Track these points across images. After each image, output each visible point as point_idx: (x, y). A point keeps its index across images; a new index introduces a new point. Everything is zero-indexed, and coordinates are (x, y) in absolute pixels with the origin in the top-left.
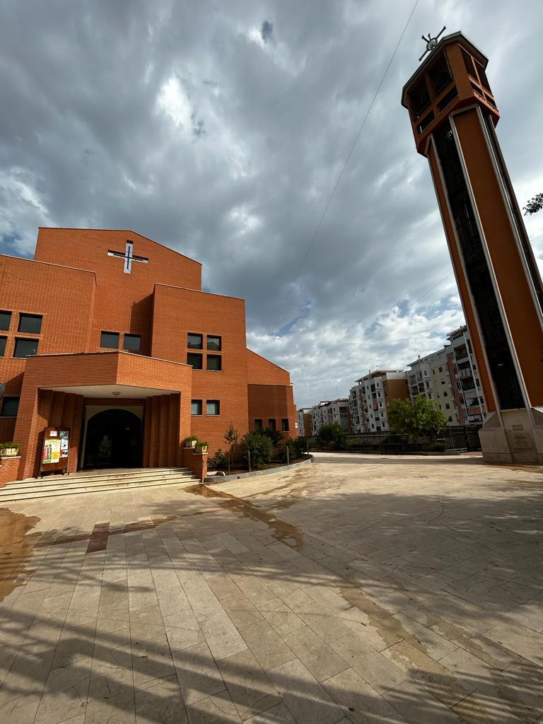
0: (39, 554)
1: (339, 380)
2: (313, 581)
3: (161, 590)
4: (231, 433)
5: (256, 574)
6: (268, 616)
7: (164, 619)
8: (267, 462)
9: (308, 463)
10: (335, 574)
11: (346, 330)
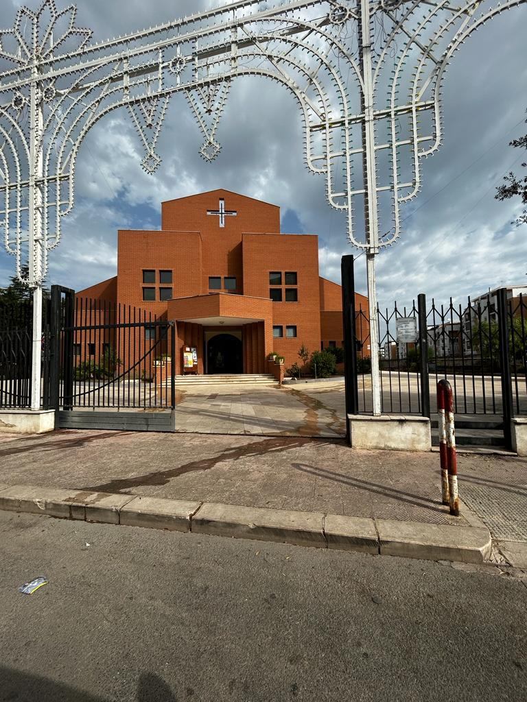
4: (303, 351)
11: (465, 237)
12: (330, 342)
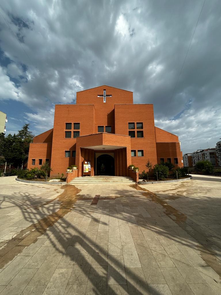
0: (78, 202)
1: (210, 139)
2: (183, 242)
3: (111, 225)
4: (148, 164)
5: (152, 229)
6: (154, 253)
7: (109, 239)
8: (166, 177)
9: (188, 179)
10: (198, 242)
11: (214, 112)
12: (168, 159)
